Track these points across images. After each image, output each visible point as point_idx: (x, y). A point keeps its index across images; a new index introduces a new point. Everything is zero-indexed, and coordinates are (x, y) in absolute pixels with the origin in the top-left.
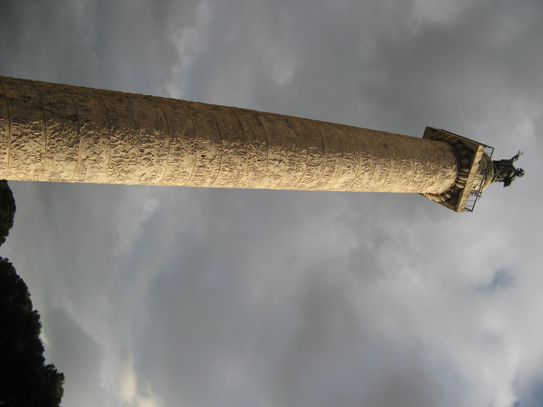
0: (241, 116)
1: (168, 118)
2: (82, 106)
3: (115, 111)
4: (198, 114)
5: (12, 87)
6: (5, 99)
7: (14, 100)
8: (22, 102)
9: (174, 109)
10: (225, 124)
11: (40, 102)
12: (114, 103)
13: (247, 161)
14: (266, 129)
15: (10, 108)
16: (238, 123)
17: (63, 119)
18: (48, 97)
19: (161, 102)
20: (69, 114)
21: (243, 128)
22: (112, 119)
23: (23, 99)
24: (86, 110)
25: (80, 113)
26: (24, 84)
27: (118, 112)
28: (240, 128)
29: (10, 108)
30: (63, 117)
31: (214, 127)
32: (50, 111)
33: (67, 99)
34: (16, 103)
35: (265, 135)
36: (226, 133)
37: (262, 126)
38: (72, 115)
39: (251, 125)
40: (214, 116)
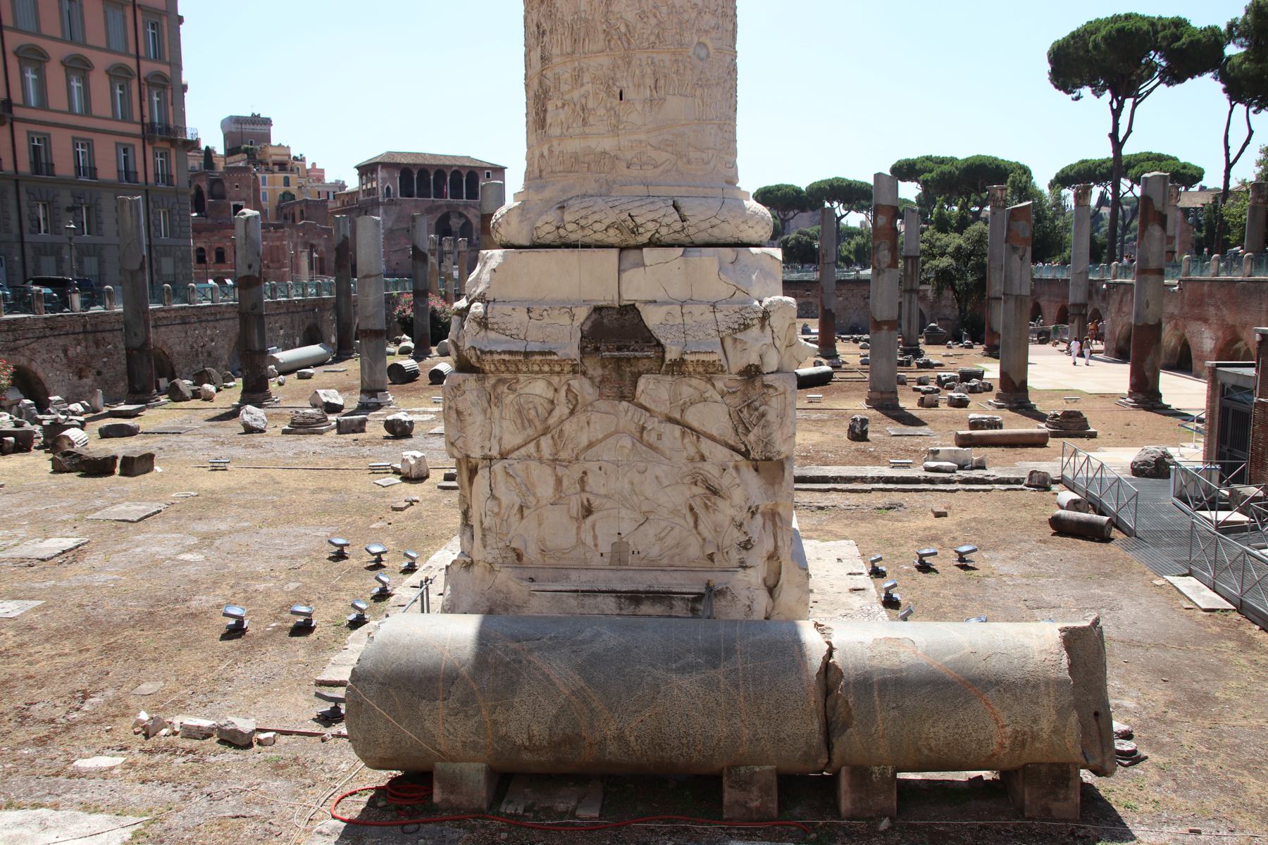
8: (546, 39)
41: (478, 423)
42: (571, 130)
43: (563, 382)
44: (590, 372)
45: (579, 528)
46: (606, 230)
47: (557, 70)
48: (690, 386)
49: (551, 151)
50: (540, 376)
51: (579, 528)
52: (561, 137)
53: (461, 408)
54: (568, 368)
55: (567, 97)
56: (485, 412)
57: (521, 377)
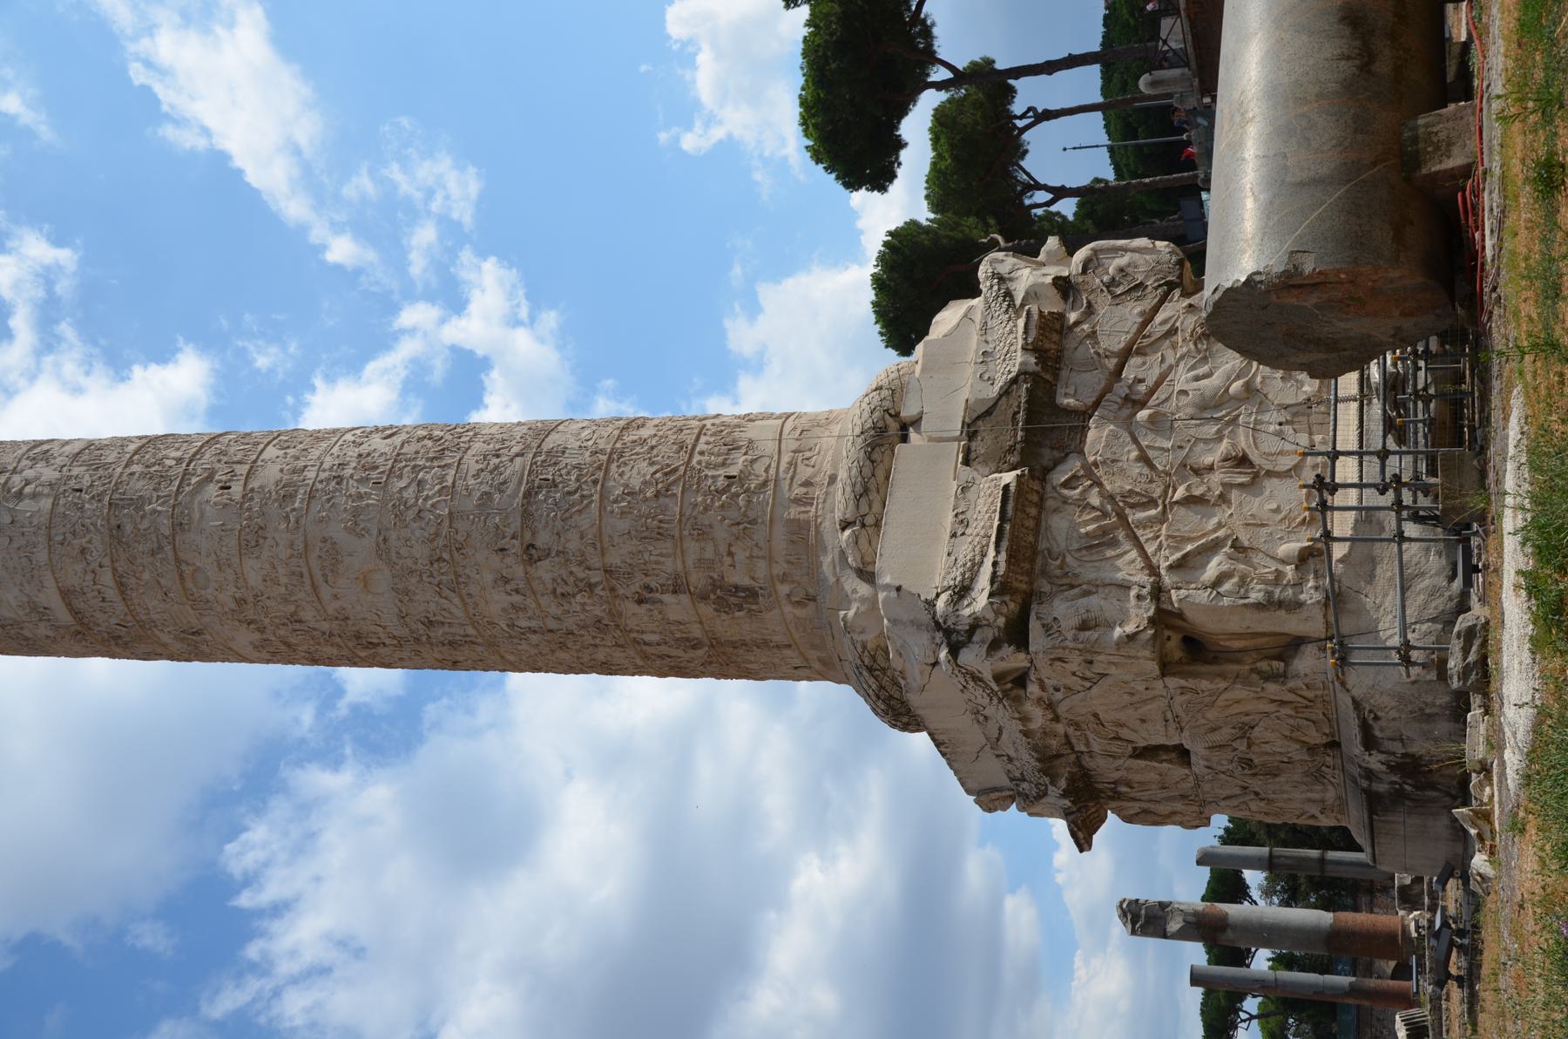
0: (122, 617)
1: (307, 581)
2: (517, 591)
3: (438, 586)
4: (233, 606)
5: (681, 627)
6: (692, 589)
7: (671, 588)
8: (653, 585)
9: (295, 612)
10: (163, 581)
11: (612, 589)
12: (443, 613)
14: (50, 582)
15: (680, 567)
17: (560, 548)
18: (598, 611)
19: (331, 634)
20: (545, 563)
22: (444, 560)
23: (651, 595)
24: (507, 581)
25: (519, 571)
26: (658, 644)
27: (430, 583)
29: (680, 567)
30: (558, 553)
32: (589, 569)
33: (554, 610)
34: (668, 579)
35: (55, 563)
37: (61, 591)
38: (538, 564)
39: (93, 591)
40: (191, 606)
41: (1102, 603)
42: (761, 544)
43: (1055, 495)
44: (1046, 462)
45: (1270, 474)
46: (873, 462)
47: (690, 563)
48: (1076, 348)
49: (784, 578)
50: (1043, 523)
51: (1270, 474)
52: (770, 560)
53: (1075, 621)
54: (1036, 485)
55: (723, 549)
56: (1086, 594)
57: (1043, 545)
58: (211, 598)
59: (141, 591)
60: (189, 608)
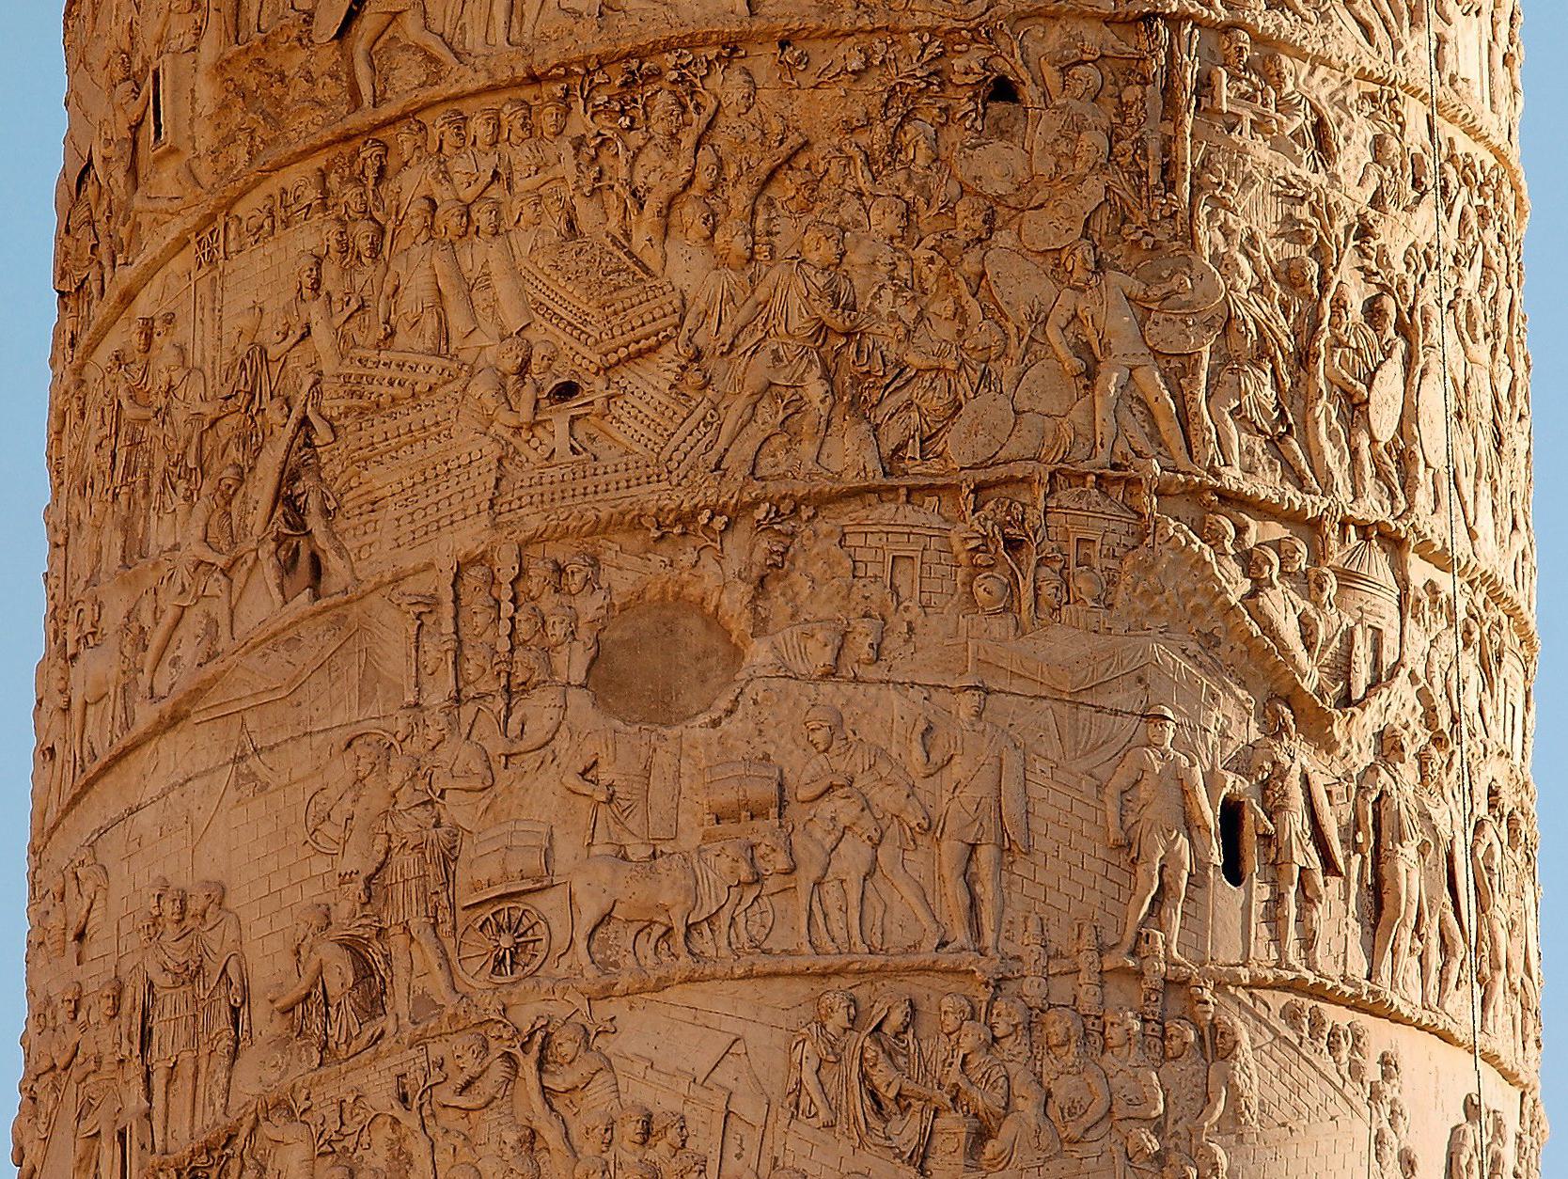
0: (411, 28)
10: (655, 377)
13: (1266, 21)
16: (580, 122)
21: (691, 42)
28: (686, 90)
31: (734, 601)
36: (815, 389)
58: (538, 712)
59: (587, 214)
60: (469, 537)
